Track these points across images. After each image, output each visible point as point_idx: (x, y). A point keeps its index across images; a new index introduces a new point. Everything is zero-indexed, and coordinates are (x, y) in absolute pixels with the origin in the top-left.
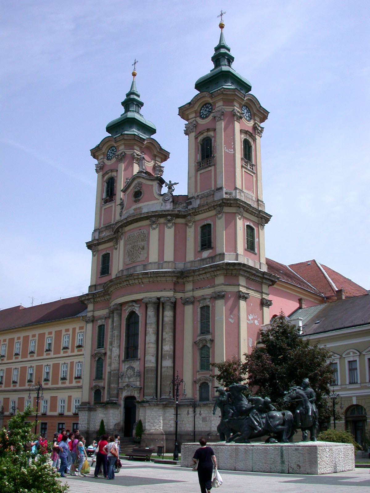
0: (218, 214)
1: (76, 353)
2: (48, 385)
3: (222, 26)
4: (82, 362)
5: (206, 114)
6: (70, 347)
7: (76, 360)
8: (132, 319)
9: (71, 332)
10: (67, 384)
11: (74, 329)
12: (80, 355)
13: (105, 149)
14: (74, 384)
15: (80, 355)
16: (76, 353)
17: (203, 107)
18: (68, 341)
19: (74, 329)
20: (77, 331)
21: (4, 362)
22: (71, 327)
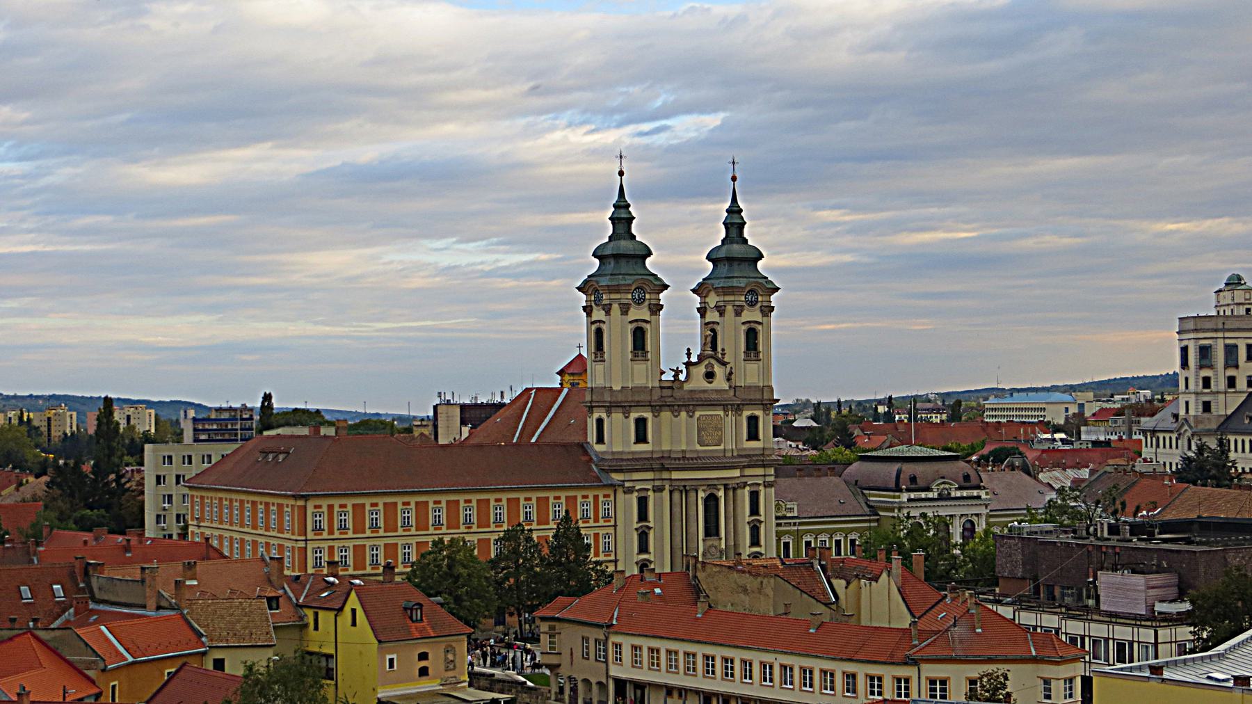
1: (601, 523)
7: (601, 532)
8: (711, 502)
20: (601, 499)
21: (472, 530)
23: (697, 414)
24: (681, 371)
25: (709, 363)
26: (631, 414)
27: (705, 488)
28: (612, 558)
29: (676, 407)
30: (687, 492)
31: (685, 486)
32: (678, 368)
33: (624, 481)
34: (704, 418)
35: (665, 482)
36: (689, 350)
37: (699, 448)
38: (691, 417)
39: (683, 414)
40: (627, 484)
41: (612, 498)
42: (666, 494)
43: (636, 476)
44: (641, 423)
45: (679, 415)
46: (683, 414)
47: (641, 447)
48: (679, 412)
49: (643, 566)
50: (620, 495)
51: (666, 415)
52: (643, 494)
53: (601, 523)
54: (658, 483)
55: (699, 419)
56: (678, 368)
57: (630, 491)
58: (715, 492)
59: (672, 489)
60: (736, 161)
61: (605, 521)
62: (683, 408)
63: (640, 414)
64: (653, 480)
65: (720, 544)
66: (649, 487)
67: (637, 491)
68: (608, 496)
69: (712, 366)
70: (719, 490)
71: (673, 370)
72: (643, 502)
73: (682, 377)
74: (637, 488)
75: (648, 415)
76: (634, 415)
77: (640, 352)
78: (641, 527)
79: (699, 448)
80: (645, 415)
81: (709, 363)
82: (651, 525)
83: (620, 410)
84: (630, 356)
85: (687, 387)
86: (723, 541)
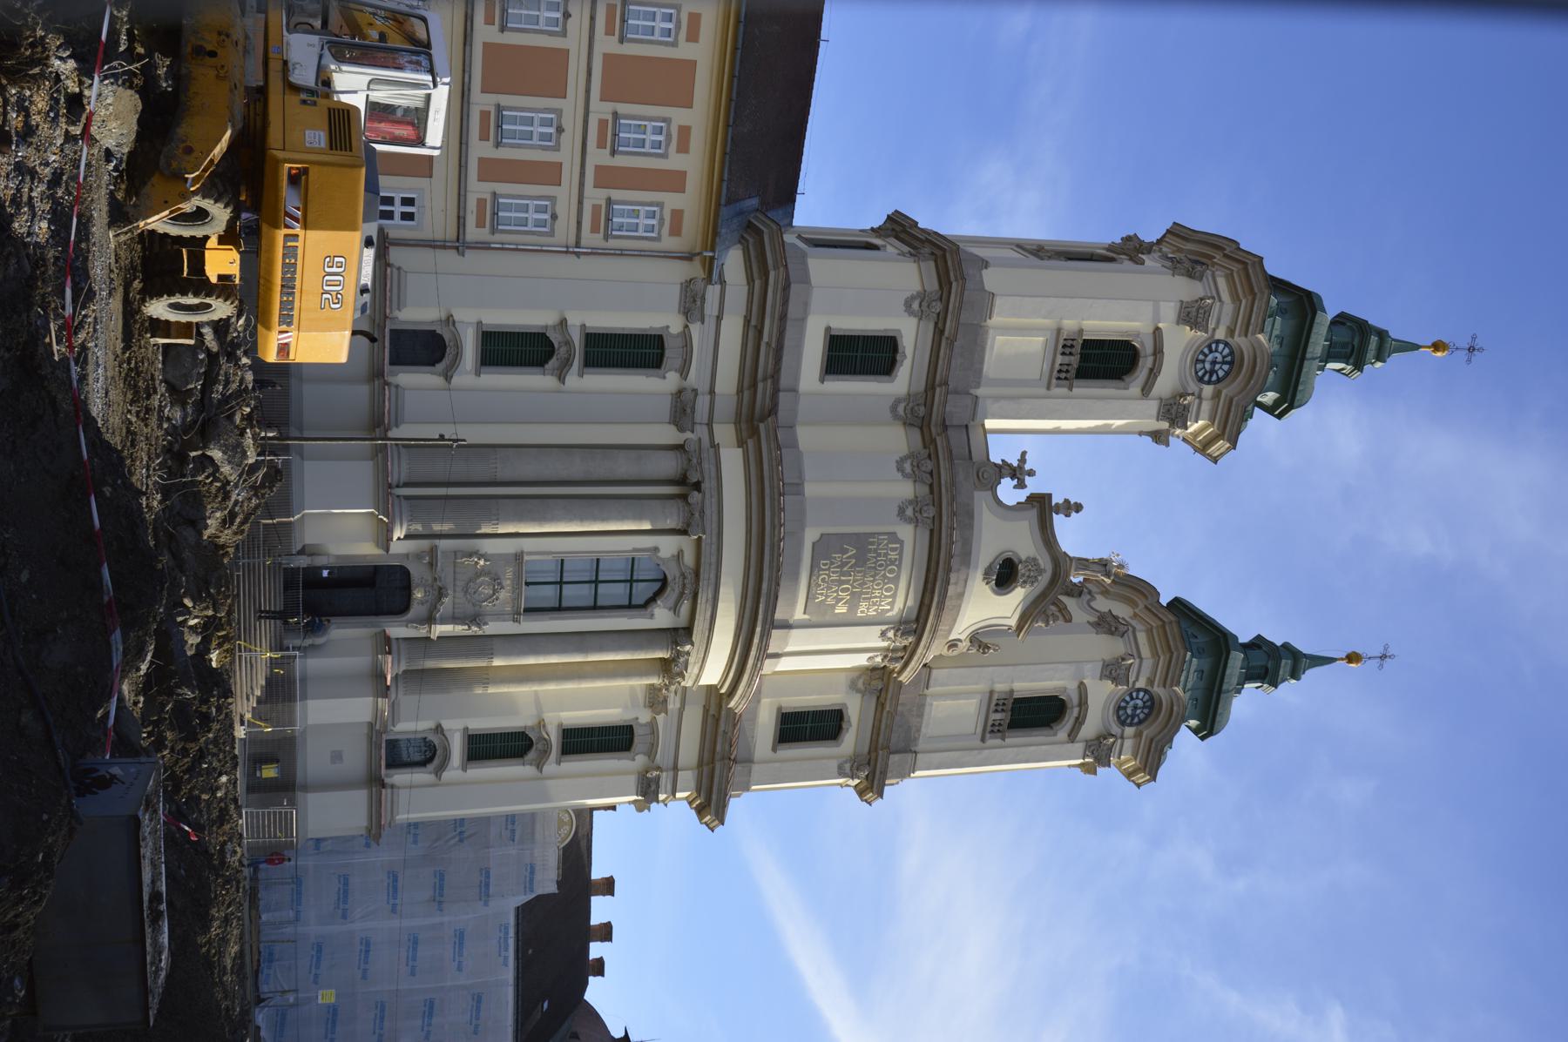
0: (852, 766)
2: (487, 23)
3: (1352, 658)
4: (552, 234)
5: (1125, 708)
6: (620, 161)
7: (564, 194)
9: (675, 162)
10: (480, 149)
11: (675, 181)
12: (579, 223)
13: (1239, 343)
14: (478, 190)
15: (579, 223)
16: (595, 196)
17: (1152, 698)
18: (642, 143)
19: (675, 181)
20: (672, 200)
22: (694, 163)
23: (906, 532)
24: (1021, 485)
25: (1041, 571)
26: (913, 321)
27: (689, 559)
28: (473, 233)
29: (929, 465)
30: (684, 497)
31: (697, 486)
32: (1031, 473)
33: (722, 282)
34: (893, 555)
36: (1078, 508)
37: (811, 535)
40: (713, 292)
41: (669, 243)
42: (669, 435)
43: (732, 330)
45: (906, 476)
47: (813, 352)
48: (915, 478)
50: (679, 272)
51: (897, 440)
52: (672, 354)
53: (595, 196)
54: (702, 403)
55: (893, 537)
56: (1031, 473)
57: (691, 305)
58: (671, 594)
59: (691, 447)
61: (596, 208)
64: (712, 392)
65: (499, 616)
67: (686, 335)
68: (676, 230)
69: (1030, 580)
70: (675, 609)
71: (1023, 460)
73: (1008, 492)
74: (695, 329)
75: (904, 380)
77: (1075, 360)
78: (568, 343)
79: (811, 535)
80: (903, 372)
81: (1041, 571)
82: (572, 380)
83: (933, 285)
84: (1070, 324)
85: (981, 499)
86: (508, 627)
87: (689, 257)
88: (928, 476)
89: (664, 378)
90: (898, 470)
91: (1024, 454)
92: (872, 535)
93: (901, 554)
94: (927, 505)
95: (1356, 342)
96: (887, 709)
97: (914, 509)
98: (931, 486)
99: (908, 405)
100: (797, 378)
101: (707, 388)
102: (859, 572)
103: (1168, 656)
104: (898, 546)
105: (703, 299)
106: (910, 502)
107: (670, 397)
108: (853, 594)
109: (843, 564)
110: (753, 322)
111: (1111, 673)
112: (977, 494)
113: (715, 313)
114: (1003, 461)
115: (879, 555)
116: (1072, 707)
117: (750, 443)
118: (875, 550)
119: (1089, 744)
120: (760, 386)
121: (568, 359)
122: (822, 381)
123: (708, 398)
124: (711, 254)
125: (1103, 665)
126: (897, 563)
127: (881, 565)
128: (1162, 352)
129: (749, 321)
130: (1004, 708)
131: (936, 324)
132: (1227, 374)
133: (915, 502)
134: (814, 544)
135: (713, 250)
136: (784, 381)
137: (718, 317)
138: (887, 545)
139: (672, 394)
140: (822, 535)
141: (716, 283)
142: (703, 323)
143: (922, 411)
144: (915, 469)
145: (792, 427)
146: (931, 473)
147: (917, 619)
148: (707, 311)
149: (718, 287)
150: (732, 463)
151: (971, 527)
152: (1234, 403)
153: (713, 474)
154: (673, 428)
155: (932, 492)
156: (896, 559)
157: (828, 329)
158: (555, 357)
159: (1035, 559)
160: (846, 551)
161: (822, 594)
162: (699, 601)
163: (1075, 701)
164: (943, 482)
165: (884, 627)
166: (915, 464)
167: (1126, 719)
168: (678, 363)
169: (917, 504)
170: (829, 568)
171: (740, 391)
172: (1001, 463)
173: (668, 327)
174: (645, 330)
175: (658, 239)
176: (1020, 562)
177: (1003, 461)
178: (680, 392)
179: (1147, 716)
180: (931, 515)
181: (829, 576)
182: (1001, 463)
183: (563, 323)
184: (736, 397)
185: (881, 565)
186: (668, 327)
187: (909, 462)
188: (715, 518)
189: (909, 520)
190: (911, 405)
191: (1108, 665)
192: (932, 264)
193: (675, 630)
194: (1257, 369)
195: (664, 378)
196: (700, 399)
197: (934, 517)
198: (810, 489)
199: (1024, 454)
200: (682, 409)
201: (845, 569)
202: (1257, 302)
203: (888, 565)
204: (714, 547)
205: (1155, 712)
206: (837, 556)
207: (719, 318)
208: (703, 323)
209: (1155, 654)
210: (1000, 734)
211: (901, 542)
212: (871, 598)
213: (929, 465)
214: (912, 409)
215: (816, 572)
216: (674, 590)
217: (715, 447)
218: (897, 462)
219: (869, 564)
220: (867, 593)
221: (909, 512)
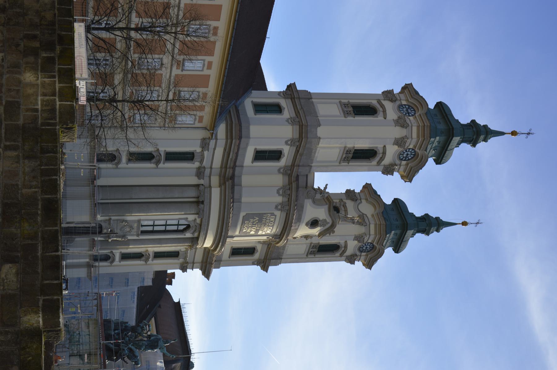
0: (257, 262)
3: (464, 224)
27: (198, 221)
29: (289, 192)
31: (202, 202)
33: (216, 139)
34: (272, 220)
35: (207, 179)
37: (242, 214)
38: (276, 207)
39: (279, 199)
40: (212, 143)
41: (197, 125)
42: (194, 180)
44: (276, 155)
45: (279, 195)
46: (279, 199)
48: (283, 196)
49: (112, 158)
50: (201, 134)
51: (279, 180)
54: (207, 171)
55: (272, 214)
57: (205, 144)
58: (191, 230)
60: (478, 225)
62: (286, 199)
63: (286, 155)
64: (211, 168)
66: (204, 164)
69: (323, 225)
70: (193, 233)
72: (188, 157)
74: (206, 153)
75: (283, 162)
76: (287, 150)
79: (242, 214)
83: (297, 136)
86: (135, 238)
87: (205, 128)
88: (288, 196)
89: (194, 164)
90: (277, 193)
91: (327, 185)
92: (265, 214)
93: (275, 219)
94: (286, 205)
95: (475, 137)
96: (271, 250)
97: (281, 206)
98: (289, 199)
99: (284, 169)
100: (243, 162)
101: (209, 166)
102: (259, 224)
103: (380, 236)
104: (274, 217)
105: (209, 144)
106: (280, 204)
107: (195, 170)
108: (256, 230)
109: (253, 222)
110: (227, 151)
111: (357, 239)
112: (306, 200)
113: (213, 147)
114: (318, 187)
115: (267, 219)
116: (342, 247)
117: (223, 187)
118: (266, 218)
119: (348, 257)
120: (228, 170)
121: (159, 160)
122: (252, 162)
123: (209, 170)
124: (212, 132)
125: (355, 236)
126: (273, 222)
127: (268, 222)
128: (385, 153)
129: (225, 150)
130: (316, 247)
131: (297, 148)
132: (412, 158)
133: (282, 204)
134: (243, 216)
135: (213, 130)
136: (238, 163)
137: (214, 149)
138: (270, 217)
139: (196, 168)
140: (246, 214)
141: (214, 139)
142: (208, 151)
143: (289, 172)
144: (284, 193)
145: (240, 177)
146: (289, 195)
147: (280, 235)
148: (210, 147)
149: (214, 141)
150: (216, 193)
151: (302, 211)
152: (412, 169)
153: (209, 197)
154: (196, 178)
155: (288, 201)
156: (273, 221)
157: (256, 149)
158: (155, 159)
159: (325, 220)
160: (256, 218)
161: (245, 230)
162: (201, 234)
163: (343, 245)
164: (292, 199)
165: (268, 237)
166: (284, 191)
167: (363, 250)
168: (199, 160)
169: (282, 205)
170: (248, 224)
171: (221, 167)
172: (317, 188)
173: (196, 150)
174: (188, 151)
175: (194, 124)
176: (320, 221)
177: (318, 187)
178: (199, 168)
179: (371, 250)
180: (287, 209)
181: (248, 225)
182: (317, 188)
183: (158, 150)
184: (220, 169)
185: (268, 222)
186: (196, 150)
187: (282, 190)
188: (208, 206)
189: (279, 210)
190: (285, 170)
191: (356, 237)
192: (298, 126)
193: (193, 238)
194: (423, 160)
195: (194, 164)
196: (206, 170)
197: (288, 210)
198: (244, 200)
199: (327, 185)
200: (200, 173)
201: (254, 223)
202: (425, 141)
203: (270, 222)
204: (207, 220)
205: (373, 251)
206: (251, 220)
207: (215, 149)
208: (208, 151)
209: (376, 234)
210: (314, 254)
211: (276, 216)
212: (263, 230)
213: (289, 192)
214: (286, 171)
215: (244, 224)
216: (192, 229)
217: (210, 187)
218: (277, 190)
219: (263, 222)
220: (262, 229)
221: (279, 207)
